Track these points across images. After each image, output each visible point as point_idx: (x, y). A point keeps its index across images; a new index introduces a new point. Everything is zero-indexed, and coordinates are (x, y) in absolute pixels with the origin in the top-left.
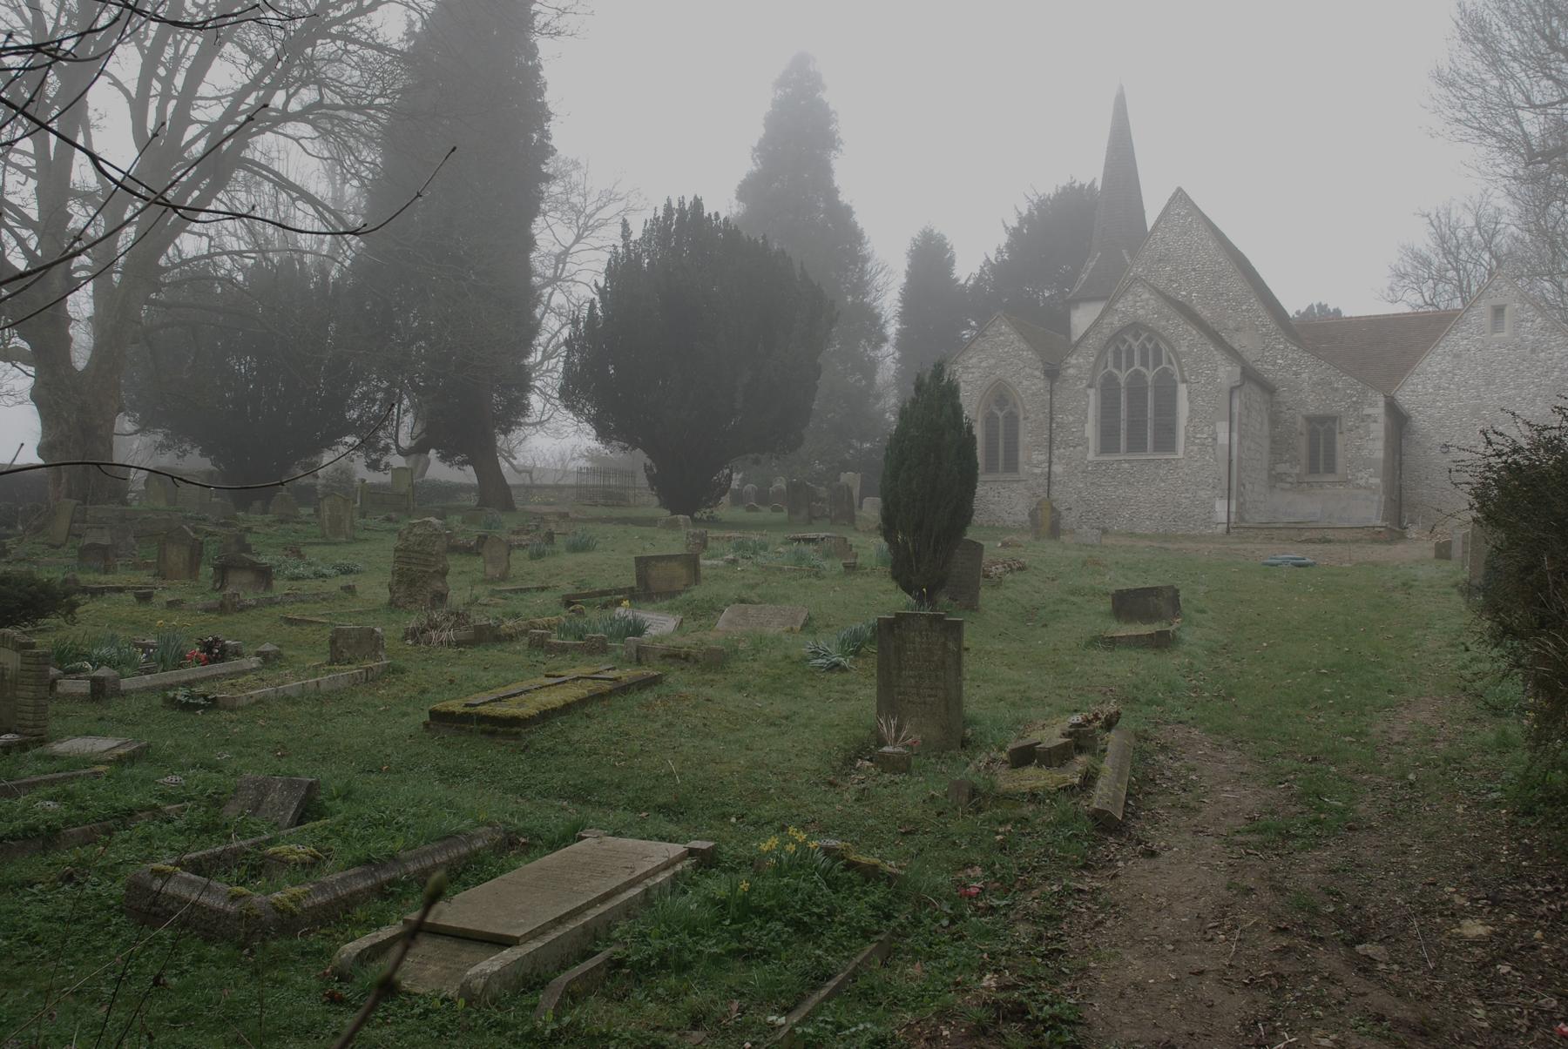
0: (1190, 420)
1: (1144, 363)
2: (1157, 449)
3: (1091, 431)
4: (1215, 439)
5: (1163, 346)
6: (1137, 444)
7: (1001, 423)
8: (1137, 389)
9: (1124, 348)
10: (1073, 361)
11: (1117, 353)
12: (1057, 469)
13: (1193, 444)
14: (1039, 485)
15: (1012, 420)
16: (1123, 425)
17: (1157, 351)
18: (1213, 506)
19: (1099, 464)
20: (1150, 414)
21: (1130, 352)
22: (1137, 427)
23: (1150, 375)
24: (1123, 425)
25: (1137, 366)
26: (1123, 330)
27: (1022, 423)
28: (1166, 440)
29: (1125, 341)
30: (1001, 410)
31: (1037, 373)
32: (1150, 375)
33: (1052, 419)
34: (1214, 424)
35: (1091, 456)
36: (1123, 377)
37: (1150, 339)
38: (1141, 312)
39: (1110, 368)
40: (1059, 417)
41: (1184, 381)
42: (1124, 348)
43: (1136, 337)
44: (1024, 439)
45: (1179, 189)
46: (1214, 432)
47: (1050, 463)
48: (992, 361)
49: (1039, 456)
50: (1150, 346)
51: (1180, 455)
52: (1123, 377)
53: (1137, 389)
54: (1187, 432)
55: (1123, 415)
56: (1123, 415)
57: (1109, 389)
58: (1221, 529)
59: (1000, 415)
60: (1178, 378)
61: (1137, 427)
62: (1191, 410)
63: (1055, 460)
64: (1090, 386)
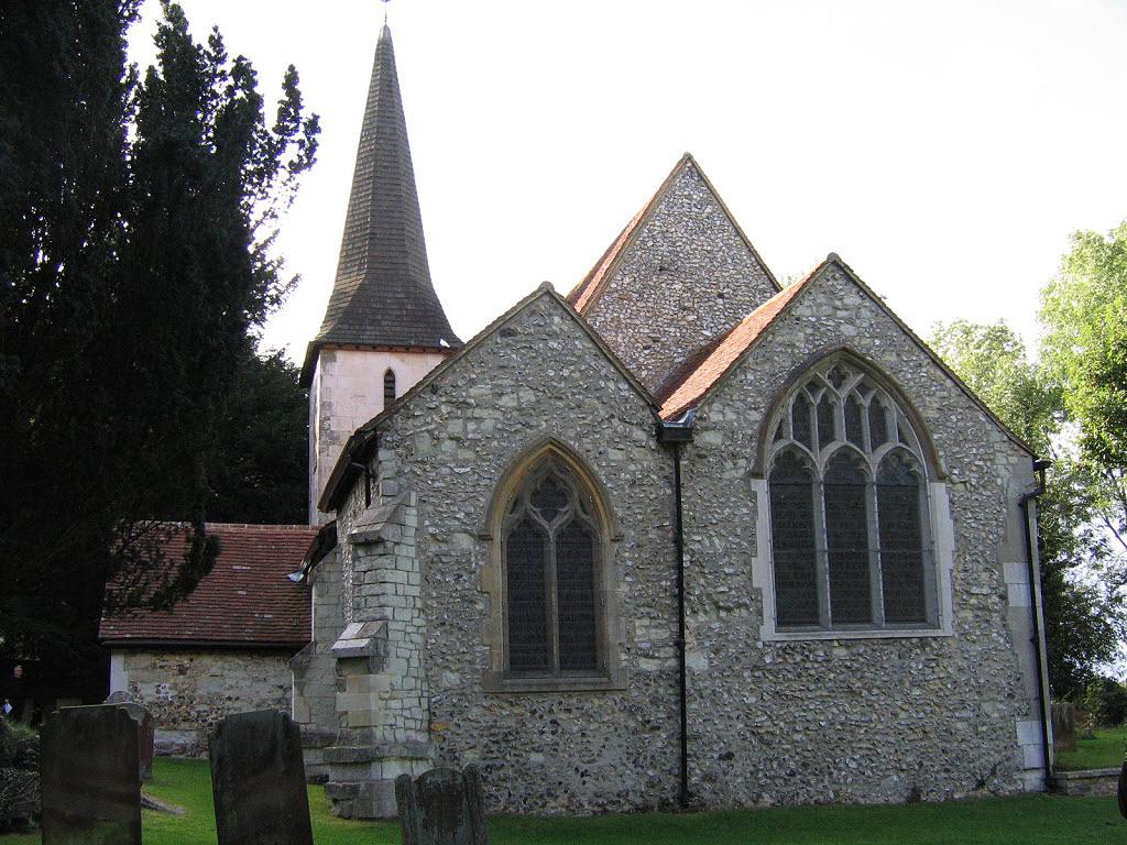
0: (959, 553)
1: (854, 433)
2: (895, 615)
3: (763, 572)
4: (1003, 597)
5: (888, 402)
6: (852, 609)
7: (552, 547)
8: (846, 482)
9: (815, 400)
10: (715, 417)
11: (801, 406)
12: (696, 661)
13: (963, 605)
14: (655, 701)
15: (582, 544)
16: (823, 564)
17: (878, 413)
18: (1013, 735)
19: (787, 650)
20: (874, 540)
21: (826, 409)
22: (849, 565)
23: (874, 460)
24: (823, 564)
25: (841, 440)
26: (816, 358)
27: (609, 551)
28: (910, 600)
29: (814, 386)
30: (550, 516)
31: (639, 434)
32: (874, 460)
33: (679, 542)
34: (999, 564)
35: (768, 630)
36: (820, 460)
37: (863, 388)
38: (848, 330)
39: (790, 437)
40: (695, 541)
41: (942, 478)
42: (815, 400)
43: (839, 379)
44: (618, 587)
45: (688, 158)
46: (1001, 582)
47: (680, 645)
48: (528, 396)
49: (650, 632)
50: (866, 402)
51: (947, 629)
52: (820, 460)
53: (846, 482)
54: (954, 580)
55: (822, 541)
56: (822, 541)
57: (789, 479)
58: (1033, 781)
59: (551, 528)
60: (922, 467)
61: (849, 565)
62: (959, 537)
63: (689, 638)
64: (756, 474)
